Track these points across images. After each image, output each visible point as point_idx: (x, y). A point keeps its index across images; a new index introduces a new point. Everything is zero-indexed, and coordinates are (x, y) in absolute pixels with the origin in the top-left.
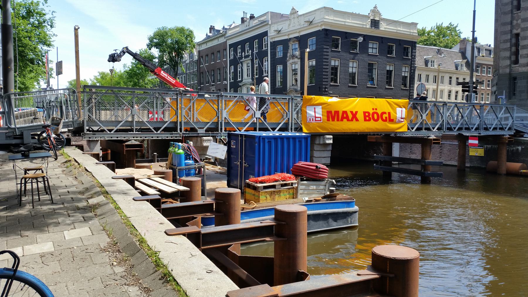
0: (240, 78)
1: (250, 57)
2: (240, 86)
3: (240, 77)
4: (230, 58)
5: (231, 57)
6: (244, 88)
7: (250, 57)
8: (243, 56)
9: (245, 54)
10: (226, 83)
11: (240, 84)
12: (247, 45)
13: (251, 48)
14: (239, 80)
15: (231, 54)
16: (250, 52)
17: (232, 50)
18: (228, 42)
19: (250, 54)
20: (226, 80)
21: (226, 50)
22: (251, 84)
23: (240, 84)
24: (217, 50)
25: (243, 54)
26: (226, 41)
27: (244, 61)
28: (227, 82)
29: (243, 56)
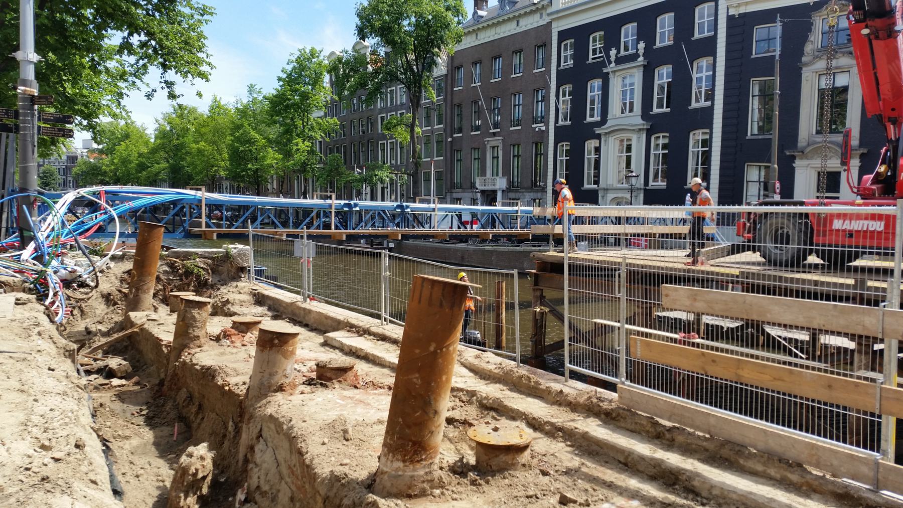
0: (592, 116)
1: (641, 59)
2: (598, 137)
3: (592, 109)
4: (559, 64)
5: (562, 64)
6: (611, 140)
7: (641, 59)
8: (613, 58)
9: (619, 52)
10: (543, 128)
11: (598, 131)
12: (629, 31)
13: (647, 33)
14: (589, 119)
15: (563, 55)
16: (642, 45)
17: (566, 45)
18: (554, 25)
19: (641, 52)
20: (544, 119)
21: (545, 45)
22: (640, 130)
23: (598, 131)
24: (512, 49)
25: (613, 52)
26: (550, 23)
27: (614, 72)
28: (547, 126)
29: (613, 58)
